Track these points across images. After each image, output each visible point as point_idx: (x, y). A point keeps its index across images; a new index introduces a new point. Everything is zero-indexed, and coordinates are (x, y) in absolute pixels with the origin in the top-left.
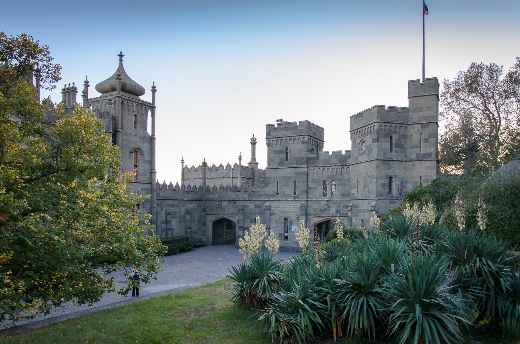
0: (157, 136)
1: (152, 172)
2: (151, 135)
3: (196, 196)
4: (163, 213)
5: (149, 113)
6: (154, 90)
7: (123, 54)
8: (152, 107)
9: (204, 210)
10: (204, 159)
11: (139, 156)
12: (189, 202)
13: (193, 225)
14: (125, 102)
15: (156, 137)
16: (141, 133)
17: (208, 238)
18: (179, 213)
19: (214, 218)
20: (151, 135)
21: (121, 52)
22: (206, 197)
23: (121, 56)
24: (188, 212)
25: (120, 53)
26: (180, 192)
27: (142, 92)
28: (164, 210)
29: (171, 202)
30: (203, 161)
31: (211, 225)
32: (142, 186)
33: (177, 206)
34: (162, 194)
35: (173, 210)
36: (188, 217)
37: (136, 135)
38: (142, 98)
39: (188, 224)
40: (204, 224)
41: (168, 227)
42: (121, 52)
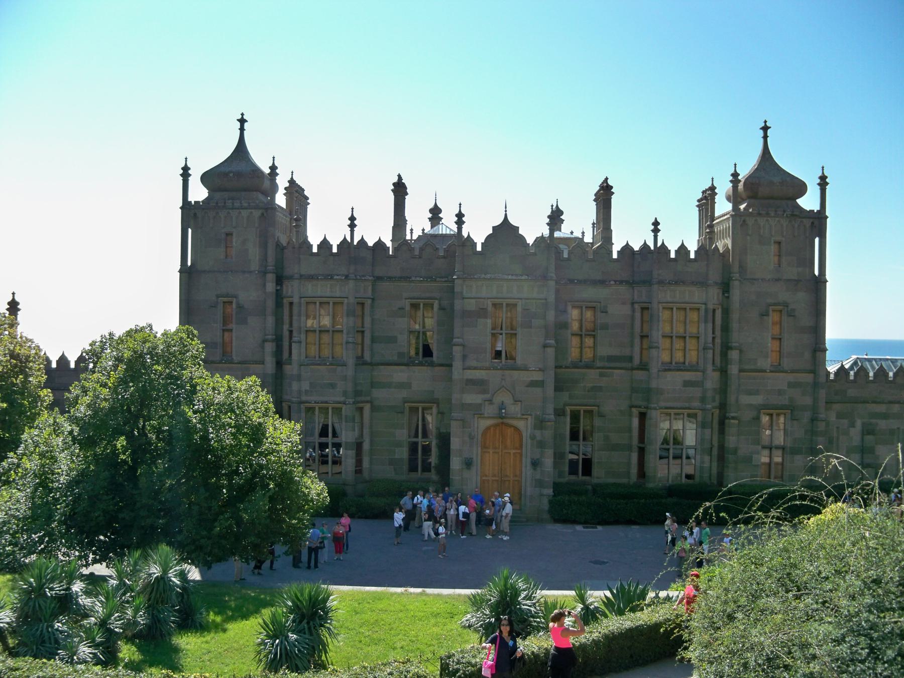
6: (823, 182)
7: (768, 124)
15: (827, 277)
16: (791, 272)
20: (816, 273)
21: (765, 122)
23: (765, 129)
25: (763, 125)
27: (801, 188)
28: (859, 423)
29: (882, 408)
32: (791, 377)
34: (852, 392)
35: (882, 424)
37: (778, 280)
42: (765, 122)
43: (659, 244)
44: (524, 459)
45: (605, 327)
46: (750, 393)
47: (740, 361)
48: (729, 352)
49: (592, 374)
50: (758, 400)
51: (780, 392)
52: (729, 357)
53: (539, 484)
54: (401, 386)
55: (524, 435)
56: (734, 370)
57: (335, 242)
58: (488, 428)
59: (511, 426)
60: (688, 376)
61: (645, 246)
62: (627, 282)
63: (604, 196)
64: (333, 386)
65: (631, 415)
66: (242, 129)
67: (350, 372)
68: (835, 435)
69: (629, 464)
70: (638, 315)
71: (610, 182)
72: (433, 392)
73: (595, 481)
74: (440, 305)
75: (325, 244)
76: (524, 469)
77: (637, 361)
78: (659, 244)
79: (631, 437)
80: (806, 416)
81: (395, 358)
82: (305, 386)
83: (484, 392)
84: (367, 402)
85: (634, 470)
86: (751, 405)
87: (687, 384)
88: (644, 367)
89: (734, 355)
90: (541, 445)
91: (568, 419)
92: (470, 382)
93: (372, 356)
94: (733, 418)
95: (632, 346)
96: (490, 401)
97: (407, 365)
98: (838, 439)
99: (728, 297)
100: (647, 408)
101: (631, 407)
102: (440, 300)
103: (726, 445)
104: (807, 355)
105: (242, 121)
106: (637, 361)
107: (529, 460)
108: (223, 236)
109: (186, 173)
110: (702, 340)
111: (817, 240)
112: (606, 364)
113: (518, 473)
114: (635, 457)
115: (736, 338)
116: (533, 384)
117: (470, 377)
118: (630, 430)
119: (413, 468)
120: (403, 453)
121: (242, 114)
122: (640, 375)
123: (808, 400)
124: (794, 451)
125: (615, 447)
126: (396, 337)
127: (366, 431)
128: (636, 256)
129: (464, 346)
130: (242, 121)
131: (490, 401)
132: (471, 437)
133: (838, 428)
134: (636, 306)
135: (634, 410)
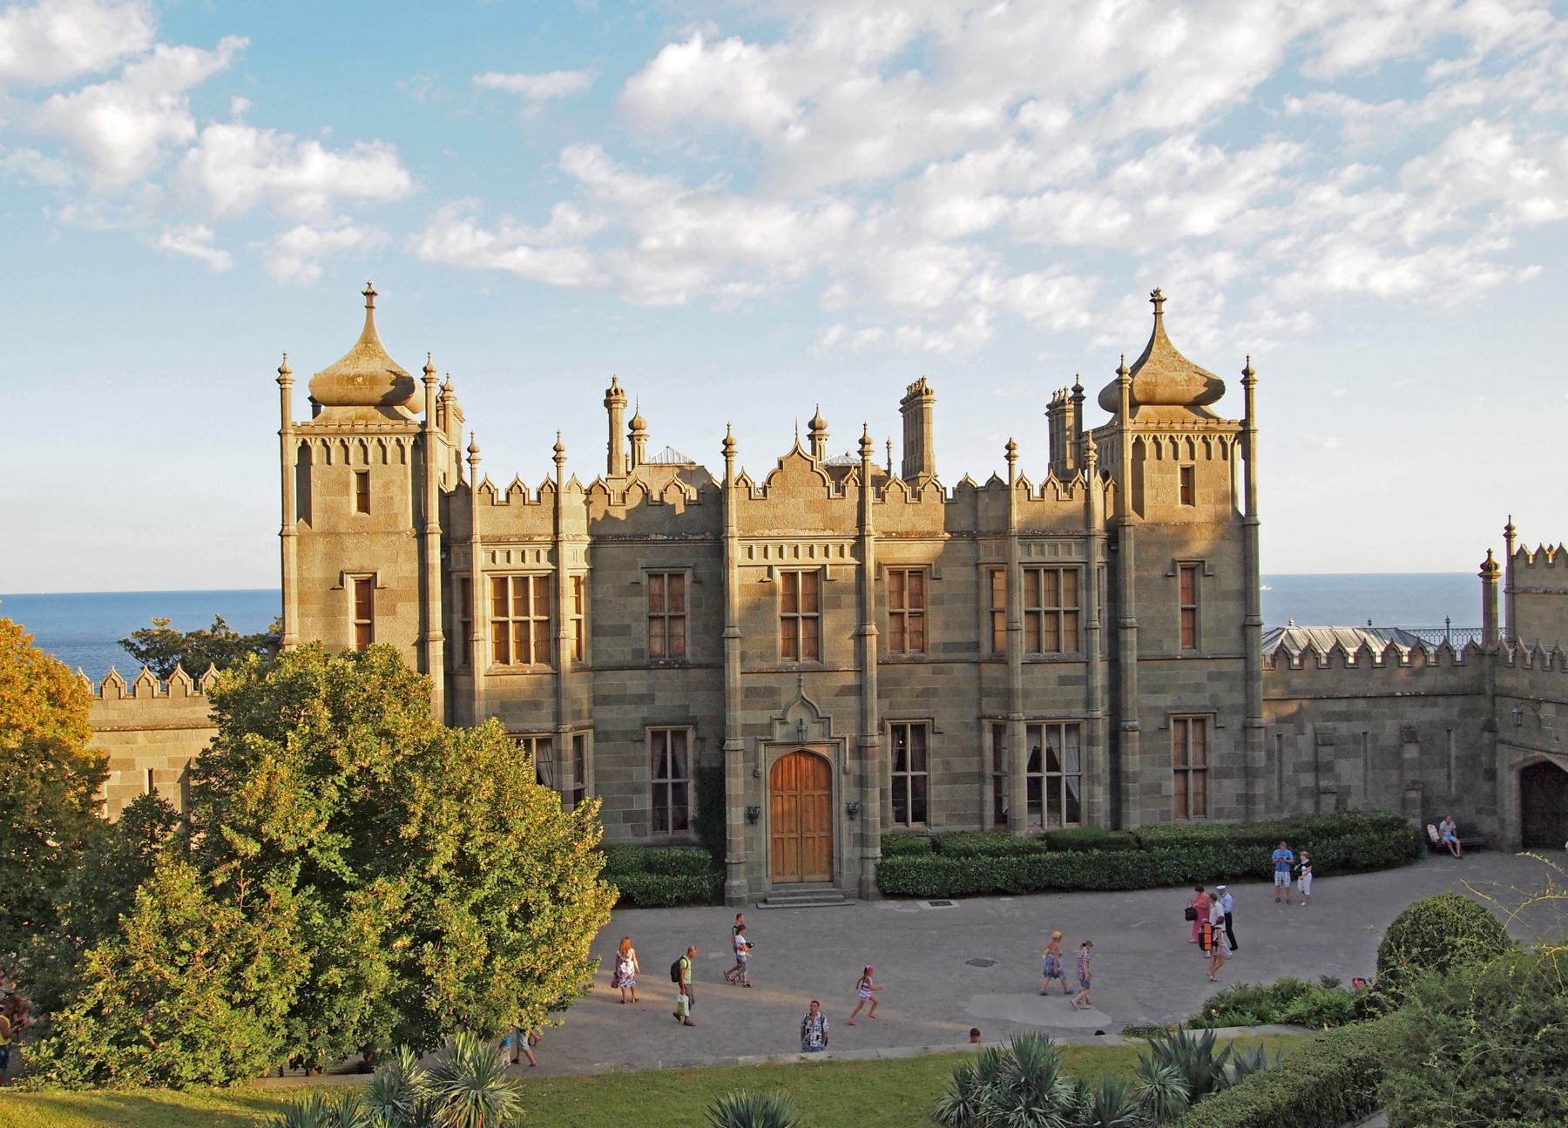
0: (1262, 514)
1: (1249, 624)
2: (1242, 511)
3: (1452, 680)
4: (1305, 742)
5: (1238, 449)
6: (1247, 378)
8: (1244, 434)
9: (1490, 727)
10: (1489, 552)
11: (1204, 585)
12: (1420, 701)
13: (1436, 777)
14: (1149, 443)
17: (1502, 821)
18: (1375, 737)
19: (1519, 758)
22: (1498, 681)
24: (1410, 735)
26: (1377, 673)
27: (1215, 390)
28: (1309, 729)
29: (1341, 706)
30: (1484, 559)
31: (1510, 782)
32: (1212, 666)
33: (1365, 716)
35: (1344, 728)
36: (1411, 752)
38: (1214, 408)
39: (1410, 776)
40: (1491, 775)
41: (1323, 784)
43: (1016, 477)
44: (835, 804)
45: (938, 601)
46: (1155, 690)
47: (1139, 644)
48: (1122, 632)
49: (923, 671)
50: (1165, 700)
51: (1198, 688)
52: (1122, 638)
53: (863, 840)
54: (640, 699)
55: (834, 767)
56: (1131, 657)
57: (532, 485)
58: (781, 760)
59: (813, 755)
60: (1065, 670)
61: (994, 481)
62: (969, 533)
63: (915, 406)
65: (980, 729)
66: (370, 307)
68: (1276, 747)
69: (981, 803)
70: (985, 581)
71: (928, 384)
72: (687, 707)
73: (933, 830)
74: (694, 576)
75: (516, 487)
76: (835, 820)
77: (986, 650)
78: (1016, 477)
79: (982, 763)
80: (1236, 722)
81: (629, 657)
83: (775, 706)
84: (589, 727)
85: (990, 812)
86: (1156, 708)
87: (1063, 681)
88: (1001, 659)
89: (1131, 637)
90: (862, 782)
92: (750, 692)
93: (594, 656)
94: (1133, 729)
95: (978, 627)
96: (783, 721)
97: (647, 668)
98: (1280, 750)
99: (1117, 551)
100: (1007, 719)
101: (980, 719)
102: (694, 568)
103: (1124, 768)
104: (1234, 632)
105: (370, 294)
106: (986, 650)
107: (844, 806)
108: (354, 478)
110: (1083, 616)
111: (1240, 464)
112: (943, 656)
113: (826, 825)
114: (989, 791)
115: (1133, 610)
116: (844, 691)
118: (980, 751)
119: (661, 824)
120: (646, 802)
122: (992, 671)
123: (1238, 699)
124: (1222, 774)
125: (956, 779)
126: (629, 627)
127: (589, 773)
128: (982, 495)
131: (783, 721)
132: (756, 775)
134: (983, 568)
135: (985, 722)
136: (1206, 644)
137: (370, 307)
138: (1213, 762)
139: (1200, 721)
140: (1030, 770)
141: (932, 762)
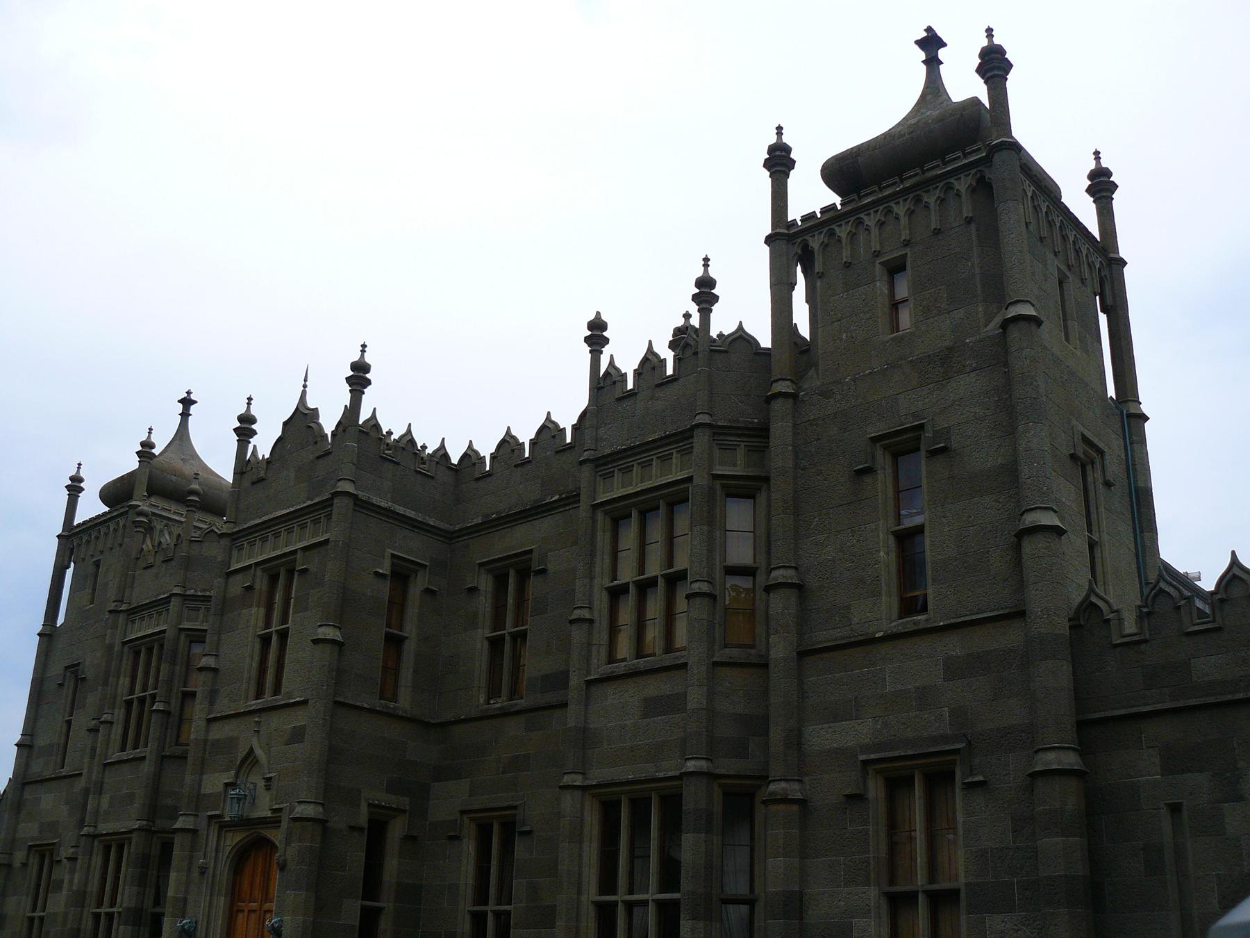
32: (953, 646)
50: (856, 734)
64: (131, 797)
66: (185, 415)
67: (147, 768)
82: (105, 802)
87: (652, 707)
91: (469, 848)
105: (187, 402)
108: (92, 569)
109: (75, 487)
117: (217, 737)
121: (189, 393)
129: (215, 670)
130: (187, 402)
133: (1175, 809)
136: (941, 601)
137: (185, 415)
138: (960, 869)
139: (939, 778)
140: (602, 892)
141: (519, 885)
